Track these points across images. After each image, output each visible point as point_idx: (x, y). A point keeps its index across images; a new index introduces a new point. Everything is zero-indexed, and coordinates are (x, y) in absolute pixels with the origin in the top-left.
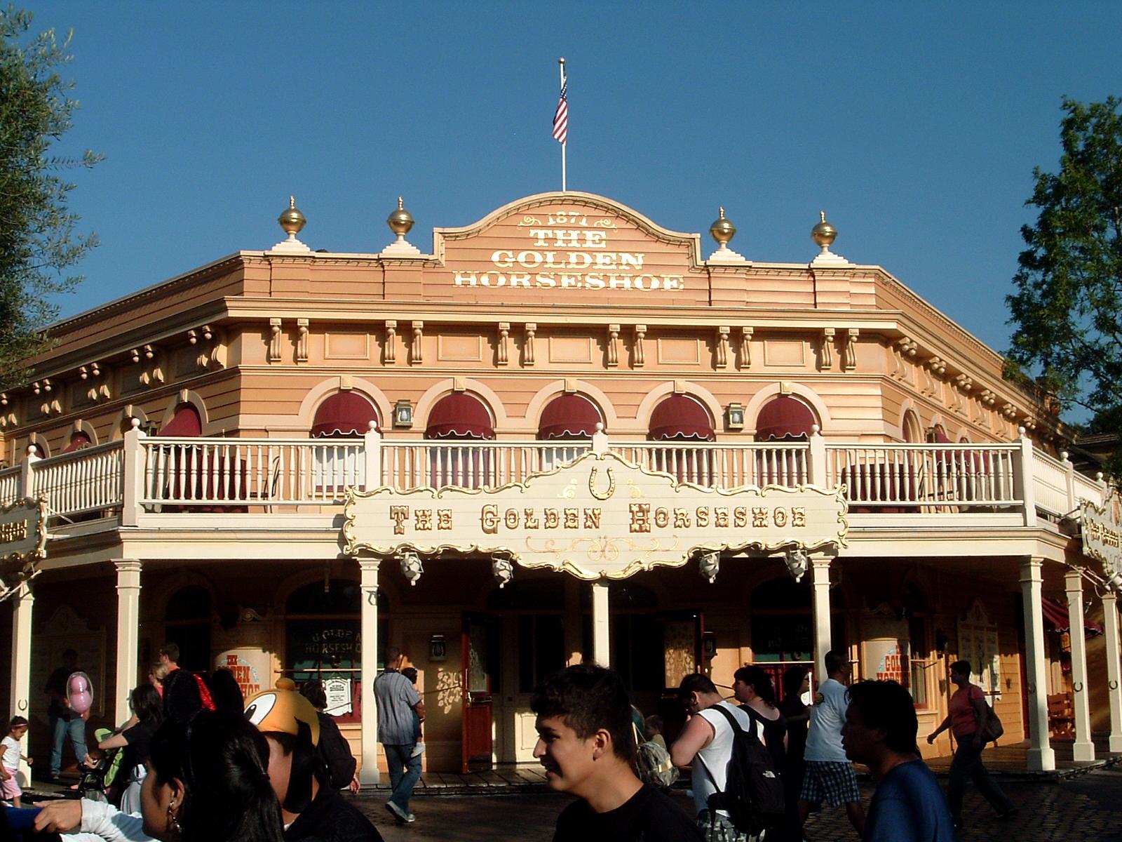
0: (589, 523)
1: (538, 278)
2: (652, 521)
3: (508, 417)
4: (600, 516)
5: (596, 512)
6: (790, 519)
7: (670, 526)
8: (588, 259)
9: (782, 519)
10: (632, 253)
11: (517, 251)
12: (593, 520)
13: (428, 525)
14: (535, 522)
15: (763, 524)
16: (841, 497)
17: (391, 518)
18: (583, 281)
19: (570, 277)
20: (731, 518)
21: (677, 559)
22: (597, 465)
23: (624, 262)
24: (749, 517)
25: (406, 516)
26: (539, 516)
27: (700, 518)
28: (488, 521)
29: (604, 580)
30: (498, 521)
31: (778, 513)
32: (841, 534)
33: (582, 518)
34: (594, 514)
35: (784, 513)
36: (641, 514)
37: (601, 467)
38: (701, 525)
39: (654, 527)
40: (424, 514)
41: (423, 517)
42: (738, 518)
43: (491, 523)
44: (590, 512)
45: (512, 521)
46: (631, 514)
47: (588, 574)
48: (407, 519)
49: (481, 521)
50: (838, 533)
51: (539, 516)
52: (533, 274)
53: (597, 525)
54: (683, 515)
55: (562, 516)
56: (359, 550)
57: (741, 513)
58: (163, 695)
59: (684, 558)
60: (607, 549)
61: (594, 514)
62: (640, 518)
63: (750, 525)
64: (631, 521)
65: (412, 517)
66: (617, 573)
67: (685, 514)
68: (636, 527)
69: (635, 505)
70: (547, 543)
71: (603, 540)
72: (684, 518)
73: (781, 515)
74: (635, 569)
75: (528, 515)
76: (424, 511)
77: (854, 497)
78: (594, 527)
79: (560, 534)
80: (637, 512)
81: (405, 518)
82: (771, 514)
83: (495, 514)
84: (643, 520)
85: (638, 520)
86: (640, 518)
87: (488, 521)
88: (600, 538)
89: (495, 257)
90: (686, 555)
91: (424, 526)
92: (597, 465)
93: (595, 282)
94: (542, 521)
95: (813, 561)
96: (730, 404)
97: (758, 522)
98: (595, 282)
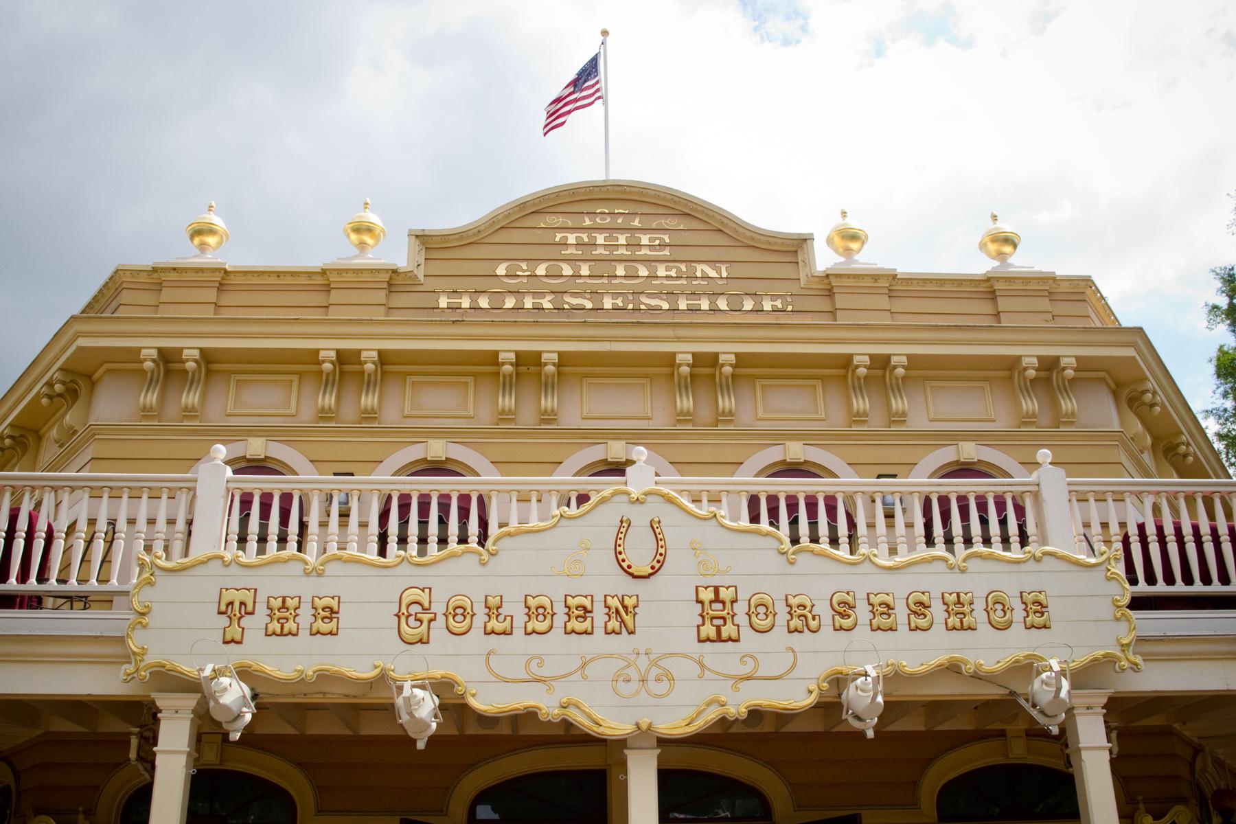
0: (614, 624)
2: (741, 619)
4: (636, 610)
5: (629, 602)
6: (1019, 614)
7: (780, 630)
9: (1002, 614)
13: (290, 626)
14: (505, 620)
17: (220, 613)
20: (901, 612)
22: (633, 513)
24: (938, 611)
25: (250, 608)
27: (839, 613)
28: (412, 619)
29: (643, 734)
30: (430, 621)
31: (997, 602)
32: (1125, 642)
33: (599, 614)
34: (625, 607)
36: (719, 606)
37: (640, 518)
39: (746, 632)
40: (284, 606)
41: (282, 611)
42: (915, 613)
43: (419, 623)
44: (614, 603)
45: (459, 618)
46: (700, 605)
47: (614, 725)
48: (252, 613)
49: (396, 618)
50: (1118, 640)
53: (630, 626)
54: (805, 607)
55: (560, 610)
56: (150, 673)
57: (922, 604)
59: (810, 692)
60: (652, 676)
61: (625, 607)
64: (700, 618)
65: (261, 610)
67: (808, 604)
69: (706, 588)
70: (528, 662)
71: (643, 658)
72: (806, 612)
73: (999, 607)
74: (712, 715)
75: (493, 610)
78: (624, 629)
80: (711, 602)
81: (247, 613)
83: (426, 605)
84: (724, 618)
85: (712, 618)
87: (412, 619)
88: (638, 654)
90: (813, 687)
91: (282, 628)
92: (633, 513)
94: (520, 619)
97: (954, 621)
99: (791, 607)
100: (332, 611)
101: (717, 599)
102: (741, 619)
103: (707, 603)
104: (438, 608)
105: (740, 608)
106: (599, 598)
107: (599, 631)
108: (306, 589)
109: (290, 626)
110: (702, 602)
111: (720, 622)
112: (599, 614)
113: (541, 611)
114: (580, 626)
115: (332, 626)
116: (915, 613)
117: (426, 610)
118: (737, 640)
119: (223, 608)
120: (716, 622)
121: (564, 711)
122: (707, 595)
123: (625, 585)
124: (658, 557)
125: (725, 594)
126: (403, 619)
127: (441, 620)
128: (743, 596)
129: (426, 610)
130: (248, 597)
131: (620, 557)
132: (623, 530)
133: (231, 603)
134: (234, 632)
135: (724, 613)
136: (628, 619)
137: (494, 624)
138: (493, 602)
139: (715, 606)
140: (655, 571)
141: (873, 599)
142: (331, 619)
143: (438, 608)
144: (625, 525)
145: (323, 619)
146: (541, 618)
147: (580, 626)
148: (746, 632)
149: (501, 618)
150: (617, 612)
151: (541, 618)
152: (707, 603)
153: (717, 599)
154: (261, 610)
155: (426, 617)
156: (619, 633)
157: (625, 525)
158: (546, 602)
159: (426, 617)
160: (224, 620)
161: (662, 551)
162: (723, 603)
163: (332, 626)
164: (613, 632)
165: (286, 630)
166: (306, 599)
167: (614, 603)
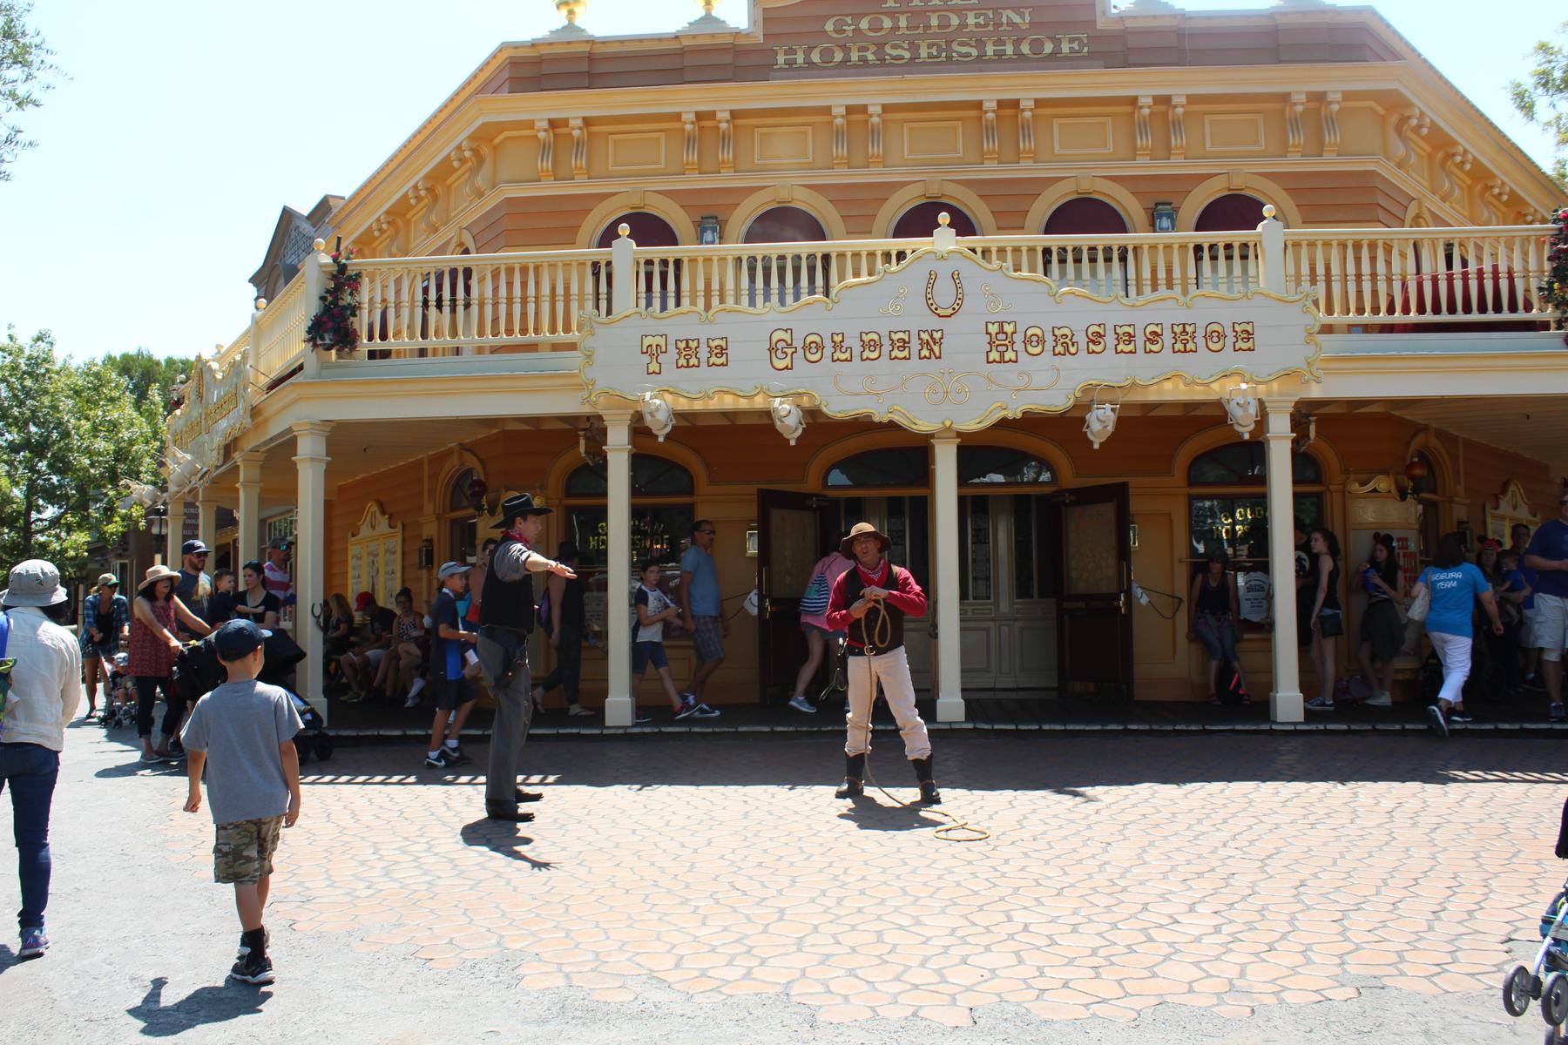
0: (925, 352)
1: (888, 49)
2: (1019, 346)
3: (847, 233)
5: (937, 336)
8: (955, 21)
10: (1016, 10)
11: (858, 17)
12: (932, 345)
15: (1188, 349)
16: (1309, 303)
18: (949, 49)
19: (930, 46)
20: (1140, 339)
21: (1056, 400)
23: (1004, 20)
25: (664, 350)
26: (853, 342)
28: (779, 352)
33: (915, 345)
35: (1220, 331)
36: (1003, 336)
38: (1093, 352)
39: (1023, 356)
41: (687, 350)
44: (925, 336)
51: (853, 342)
52: (880, 46)
53: (938, 354)
55: (886, 342)
58: (209, 608)
62: (1000, 342)
63: (1168, 350)
65: (672, 348)
66: (973, 421)
67: (1069, 334)
68: (994, 355)
75: (837, 346)
76: (687, 341)
77: (1330, 311)
79: (884, 369)
82: (1200, 333)
83: (789, 342)
84: (1006, 345)
86: (1000, 342)
87: (779, 351)
89: (829, 26)
91: (688, 362)
93: (964, 50)
94: (857, 349)
95: (1267, 405)
96: (1157, 204)
98: (964, 50)
99: (1175, 333)
100: (722, 349)
101: (1002, 331)
102: (1019, 346)
103: (993, 336)
104: (798, 344)
105: (1019, 338)
106: (1167, 326)
107: (1140, 351)
108: (702, 332)
109: (1190, 346)
110: (990, 334)
111: (1004, 348)
112: (915, 345)
113: (872, 343)
114: (1245, 346)
115: (1250, 344)
116: (1149, 339)
117: (790, 345)
118: (1016, 362)
119: (645, 350)
120: (1000, 348)
121: (890, 415)
122: (993, 329)
123: (933, 322)
124: (958, 301)
125: (1008, 329)
126: (807, 349)
127: (800, 351)
128: (1021, 329)
129: (790, 345)
130: (662, 341)
131: (930, 302)
132: (932, 281)
133: (651, 345)
134: (654, 367)
135: (1006, 342)
136: (936, 348)
137: (838, 355)
138: (838, 339)
139: (1000, 336)
140: (955, 312)
141: (1118, 330)
142: (1249, 339)
143: (798, 344)
144: (932, 278)
145: (898, 347)
146: (872, 348)
147: (1245, 346)
148: (1023, 356)
149: (843, 349)
150: (928, 343)
151: (872, 348)
152: (993, 336)
153: (1002, 331)
154: (672, 348)
155: (789, 351)
156: (930, 358)
157: (932, 278)
158: (875, 337)
159: (789, 351)
160: (646, 358)
161: (960, 296)
162: (1006, 333)
163: (1250, 344)
164: (1060, 353)
165: (691, 364)
166: (703, 341)
167: (925, 336)
